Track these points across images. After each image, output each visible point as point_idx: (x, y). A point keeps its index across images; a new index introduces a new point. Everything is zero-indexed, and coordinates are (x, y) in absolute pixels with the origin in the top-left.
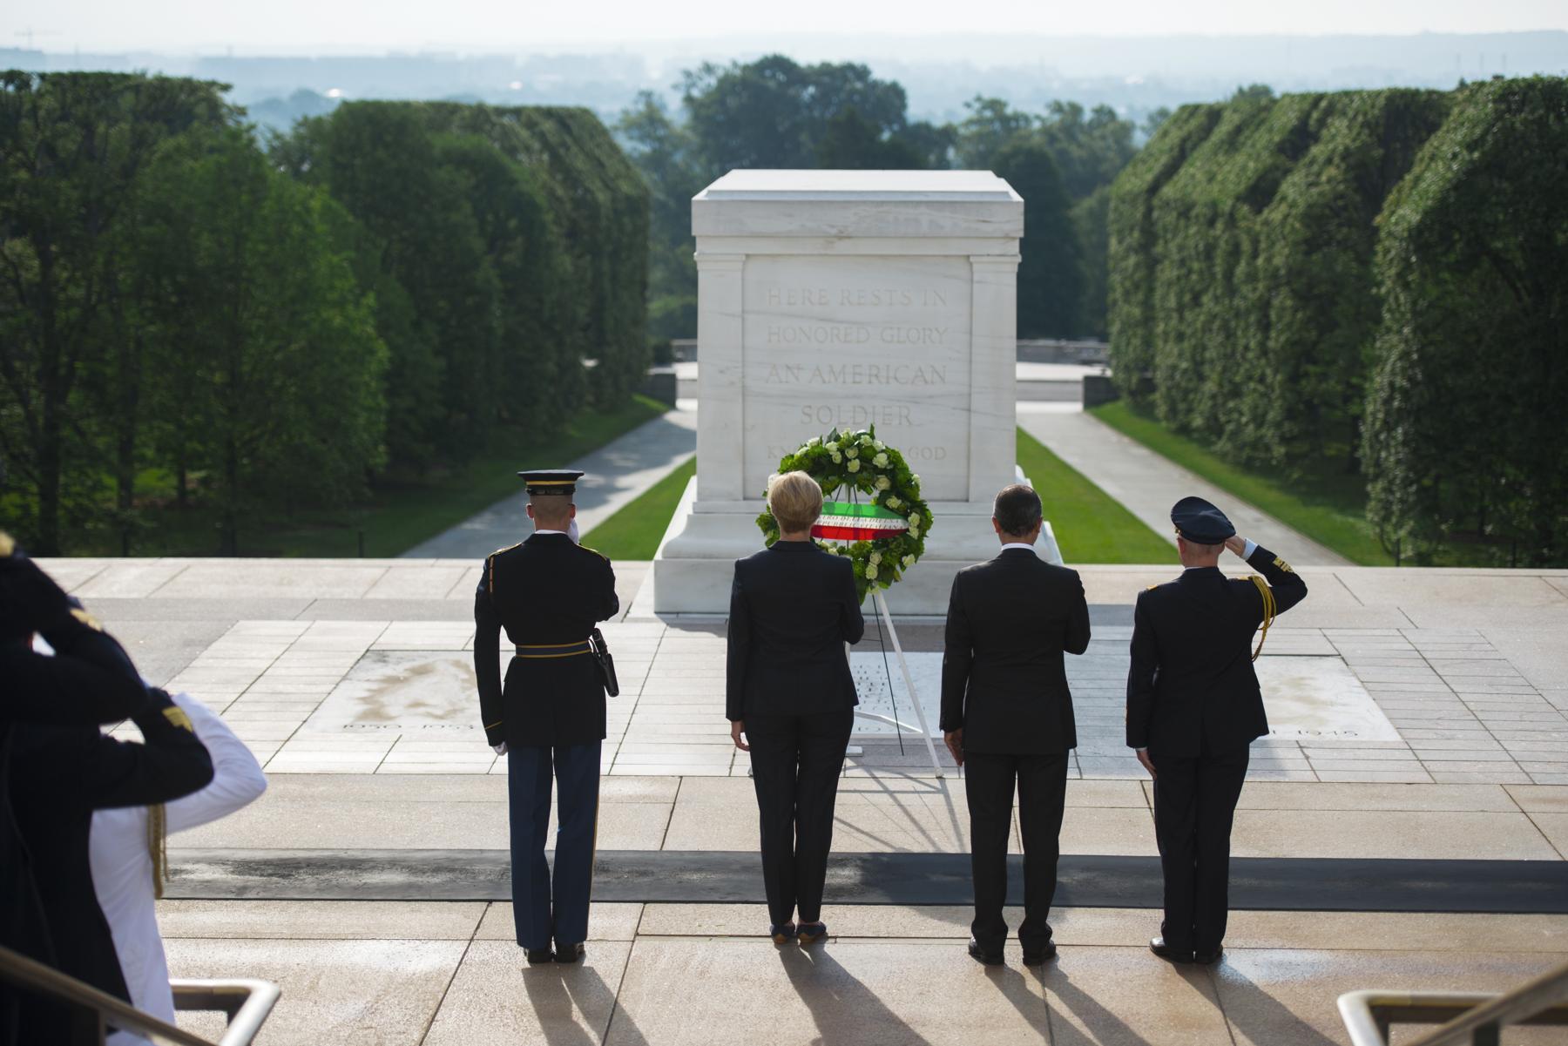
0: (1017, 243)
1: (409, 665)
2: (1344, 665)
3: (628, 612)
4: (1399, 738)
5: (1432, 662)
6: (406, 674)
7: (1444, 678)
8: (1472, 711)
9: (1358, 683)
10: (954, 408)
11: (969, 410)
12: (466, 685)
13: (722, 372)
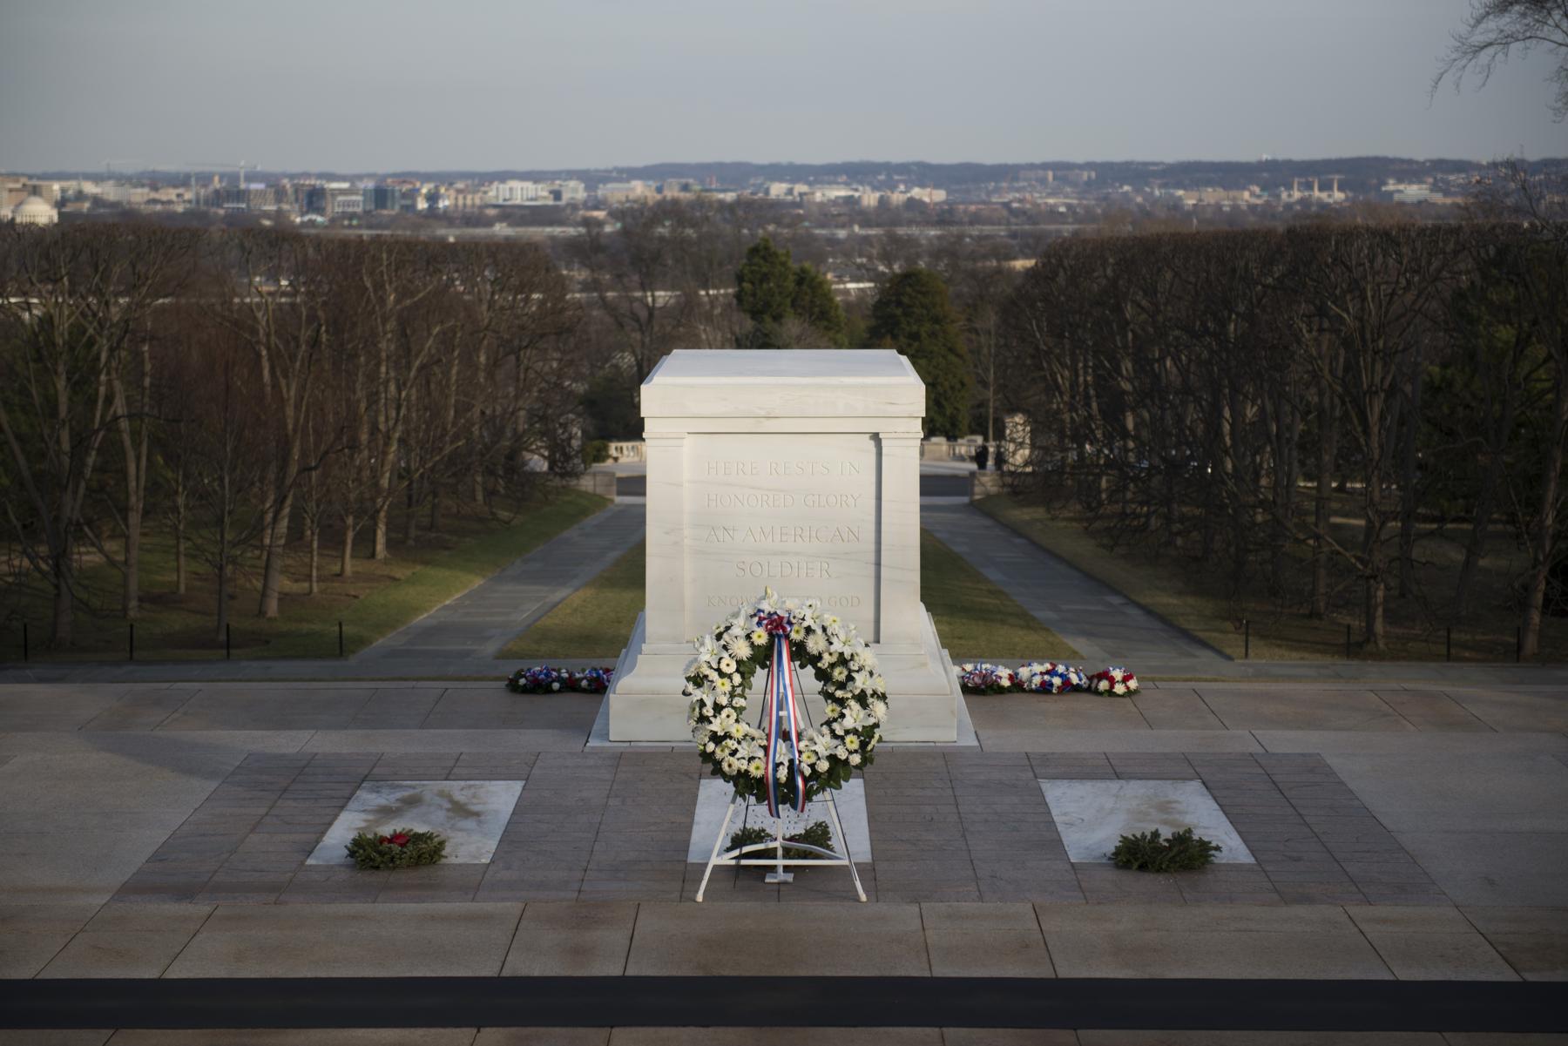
0: (919, 421)
1: (399, 795)
2: (1204, 789)
3: (587, 741)
4: (1251, 860)
5: (1280, 785)
6: (398, 805)
7: (1292, 801)
8: (1315, 833)
9: (1217, 807)
10: (867, 563)
12: (450, 814)
13: (667, 533)
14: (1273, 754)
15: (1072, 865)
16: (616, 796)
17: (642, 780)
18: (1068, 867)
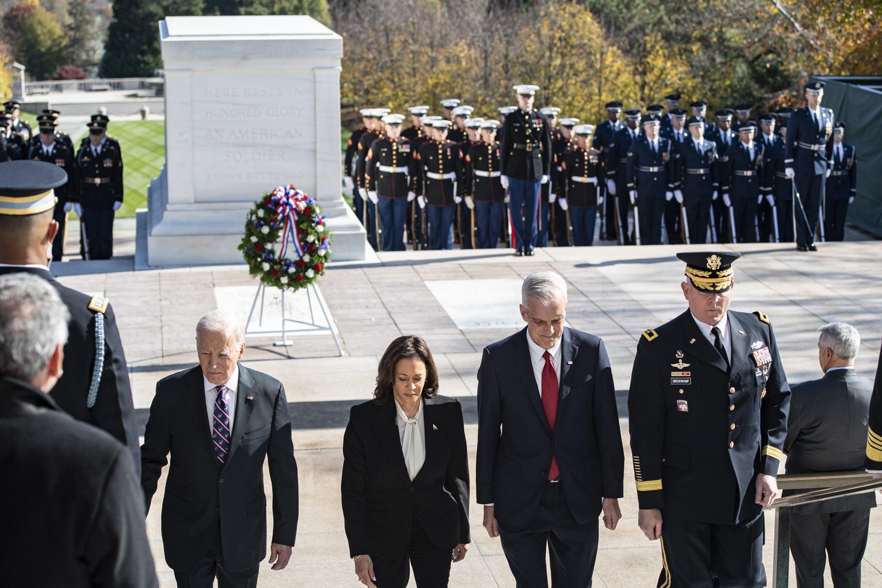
11: (315, 151)
14: (560, 262)
15: (461, 330)
16: (165, 299)
17: (178, 289)
18: (460, 332)
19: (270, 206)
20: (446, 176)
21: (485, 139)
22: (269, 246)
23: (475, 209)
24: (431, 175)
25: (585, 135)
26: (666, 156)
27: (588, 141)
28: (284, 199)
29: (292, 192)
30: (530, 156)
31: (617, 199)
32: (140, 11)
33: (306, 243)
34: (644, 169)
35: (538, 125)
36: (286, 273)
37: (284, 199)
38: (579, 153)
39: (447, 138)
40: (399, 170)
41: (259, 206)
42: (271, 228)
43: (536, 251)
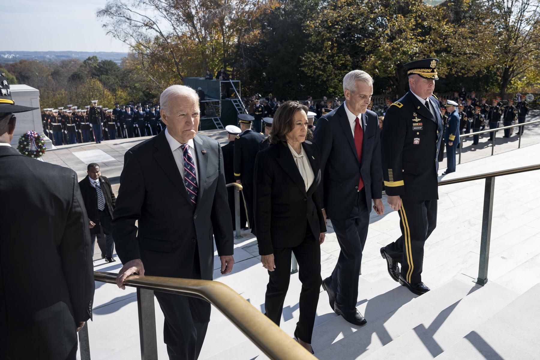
11: (33, 121)
19: (26, 137)
20: (73, 125)
21: (83, 114)
22: (27, 147)
23: (82, 133)
24: (68, 125)
25: (111, 112)
26: (133, 116)
27: (112, 113)
28: (31, 134)
29: (33, 132)
30: (98, 118)
31: (120, 128)
32: (119, 95)
33: (38, 146)
34: (127, 119)
35: (99, 110)
36: (33, 154)
37: (31, 134)
38: (110, 117)
39: (72, 115)
40: (59, 124)
41: (22, 137)
42: (27, 143)
43: (102, 142)
